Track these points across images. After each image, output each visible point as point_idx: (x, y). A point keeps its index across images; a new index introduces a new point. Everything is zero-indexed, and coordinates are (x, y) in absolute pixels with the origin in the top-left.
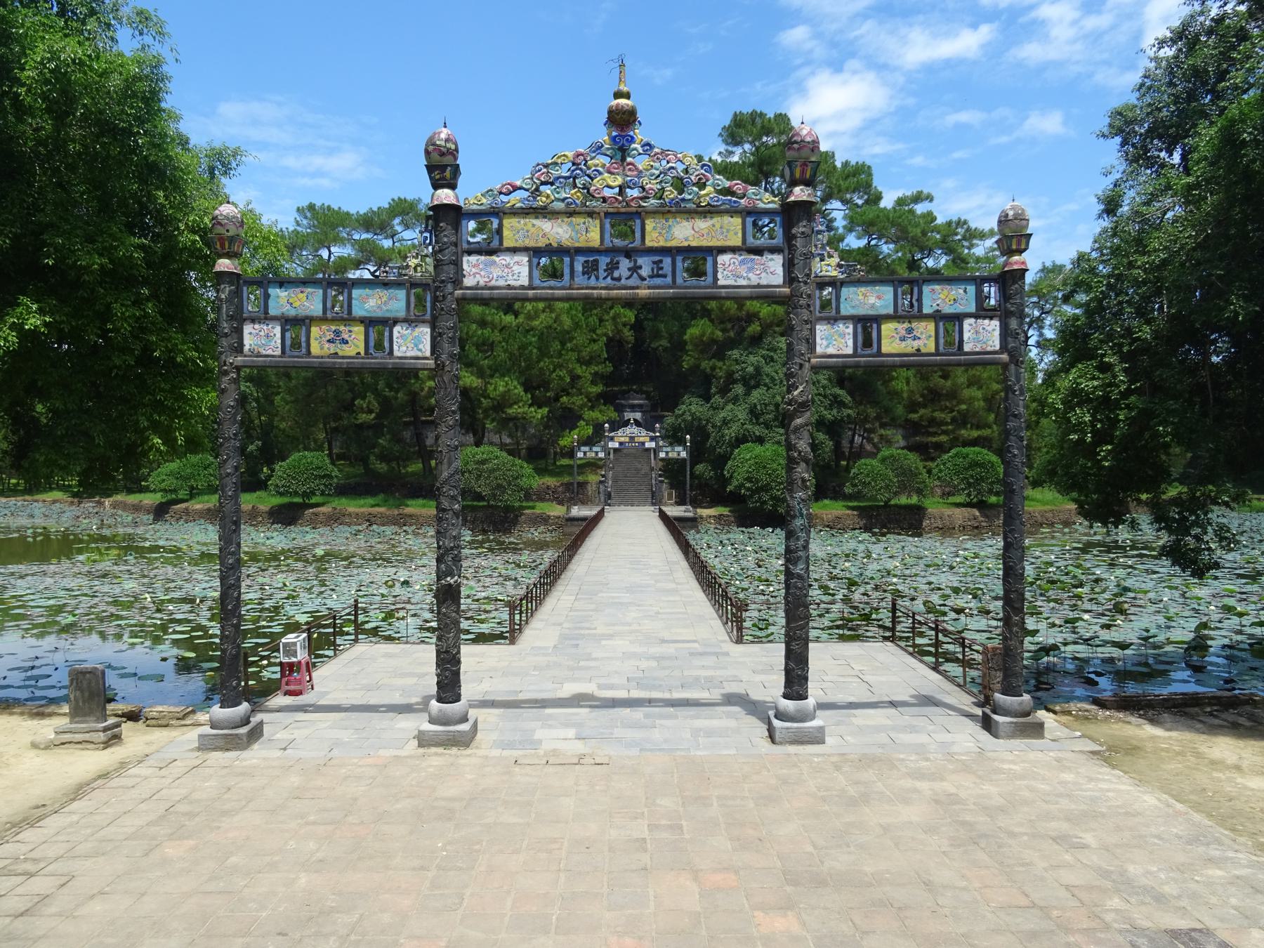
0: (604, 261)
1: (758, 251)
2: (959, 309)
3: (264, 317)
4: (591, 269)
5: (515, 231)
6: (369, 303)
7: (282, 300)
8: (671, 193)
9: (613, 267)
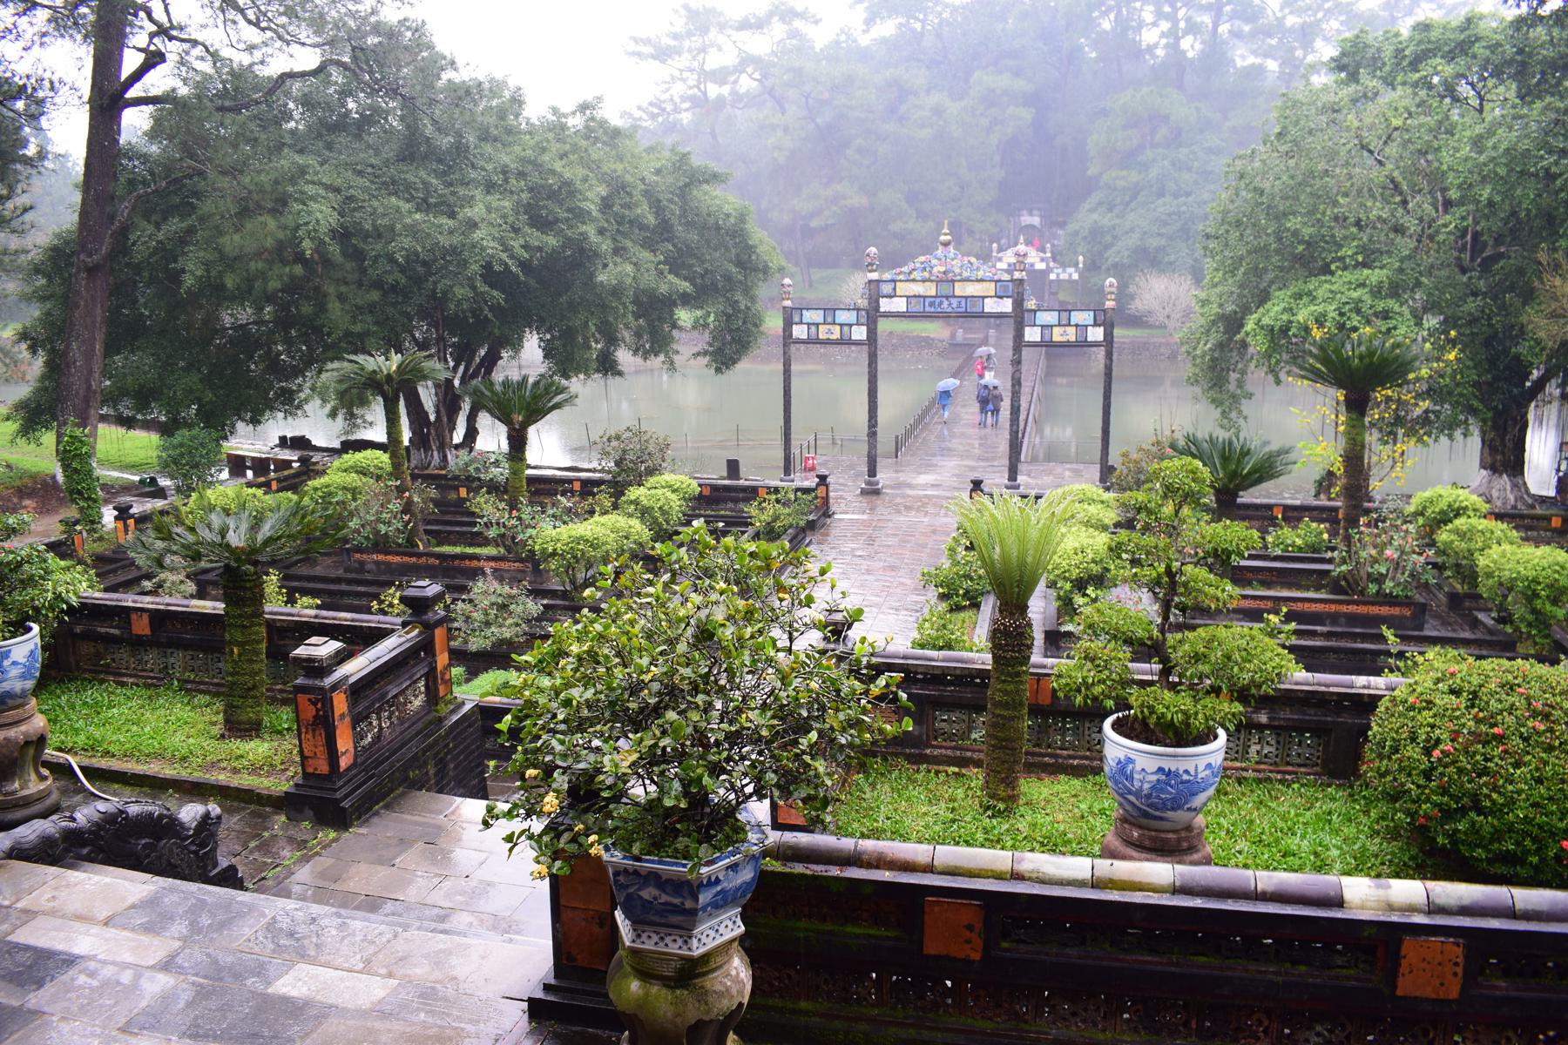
0: (938, 300)
1: (1001, 297)
3: (801, 323)
4: (931, 304)
5: (902, 288)
6: (843, 317)
7: (809, 316)
9: (941, 303)
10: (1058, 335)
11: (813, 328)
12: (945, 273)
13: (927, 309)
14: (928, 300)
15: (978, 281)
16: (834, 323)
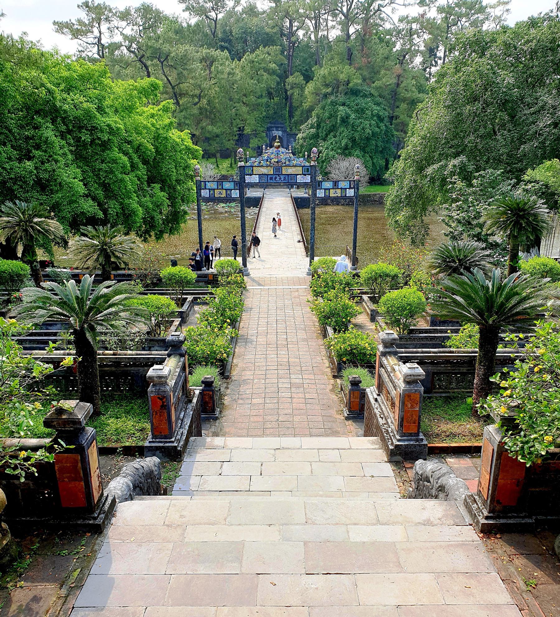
0: (274, 176)
1: (305, 175)
2: (346, 187)
4: (271, 179)
8: (287, 163)
9: (276, 178)
10: (332, 194)
11: (212, 192)
12: (277, 162)
13: (269, 181)
14: (269, 176)
15: (293, 166)
16: (223, 189)
